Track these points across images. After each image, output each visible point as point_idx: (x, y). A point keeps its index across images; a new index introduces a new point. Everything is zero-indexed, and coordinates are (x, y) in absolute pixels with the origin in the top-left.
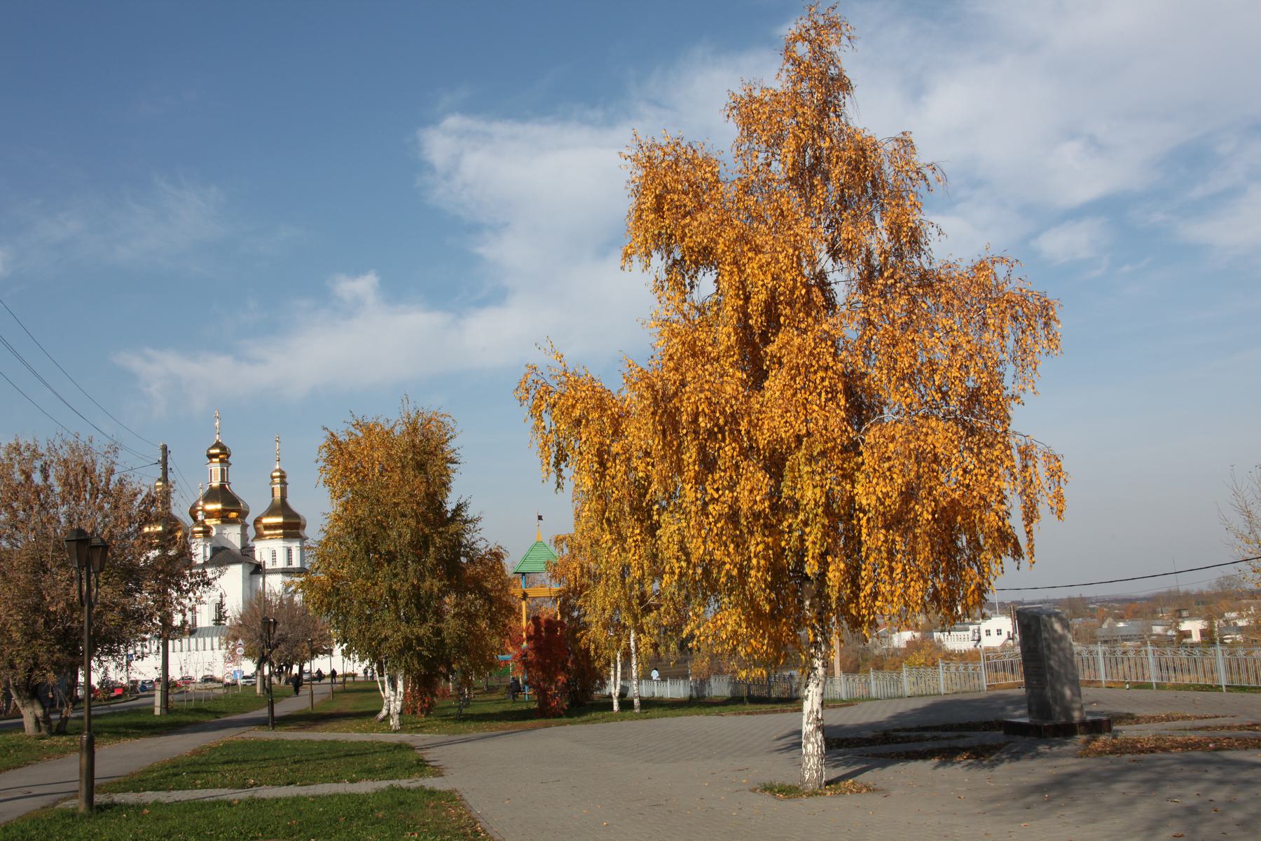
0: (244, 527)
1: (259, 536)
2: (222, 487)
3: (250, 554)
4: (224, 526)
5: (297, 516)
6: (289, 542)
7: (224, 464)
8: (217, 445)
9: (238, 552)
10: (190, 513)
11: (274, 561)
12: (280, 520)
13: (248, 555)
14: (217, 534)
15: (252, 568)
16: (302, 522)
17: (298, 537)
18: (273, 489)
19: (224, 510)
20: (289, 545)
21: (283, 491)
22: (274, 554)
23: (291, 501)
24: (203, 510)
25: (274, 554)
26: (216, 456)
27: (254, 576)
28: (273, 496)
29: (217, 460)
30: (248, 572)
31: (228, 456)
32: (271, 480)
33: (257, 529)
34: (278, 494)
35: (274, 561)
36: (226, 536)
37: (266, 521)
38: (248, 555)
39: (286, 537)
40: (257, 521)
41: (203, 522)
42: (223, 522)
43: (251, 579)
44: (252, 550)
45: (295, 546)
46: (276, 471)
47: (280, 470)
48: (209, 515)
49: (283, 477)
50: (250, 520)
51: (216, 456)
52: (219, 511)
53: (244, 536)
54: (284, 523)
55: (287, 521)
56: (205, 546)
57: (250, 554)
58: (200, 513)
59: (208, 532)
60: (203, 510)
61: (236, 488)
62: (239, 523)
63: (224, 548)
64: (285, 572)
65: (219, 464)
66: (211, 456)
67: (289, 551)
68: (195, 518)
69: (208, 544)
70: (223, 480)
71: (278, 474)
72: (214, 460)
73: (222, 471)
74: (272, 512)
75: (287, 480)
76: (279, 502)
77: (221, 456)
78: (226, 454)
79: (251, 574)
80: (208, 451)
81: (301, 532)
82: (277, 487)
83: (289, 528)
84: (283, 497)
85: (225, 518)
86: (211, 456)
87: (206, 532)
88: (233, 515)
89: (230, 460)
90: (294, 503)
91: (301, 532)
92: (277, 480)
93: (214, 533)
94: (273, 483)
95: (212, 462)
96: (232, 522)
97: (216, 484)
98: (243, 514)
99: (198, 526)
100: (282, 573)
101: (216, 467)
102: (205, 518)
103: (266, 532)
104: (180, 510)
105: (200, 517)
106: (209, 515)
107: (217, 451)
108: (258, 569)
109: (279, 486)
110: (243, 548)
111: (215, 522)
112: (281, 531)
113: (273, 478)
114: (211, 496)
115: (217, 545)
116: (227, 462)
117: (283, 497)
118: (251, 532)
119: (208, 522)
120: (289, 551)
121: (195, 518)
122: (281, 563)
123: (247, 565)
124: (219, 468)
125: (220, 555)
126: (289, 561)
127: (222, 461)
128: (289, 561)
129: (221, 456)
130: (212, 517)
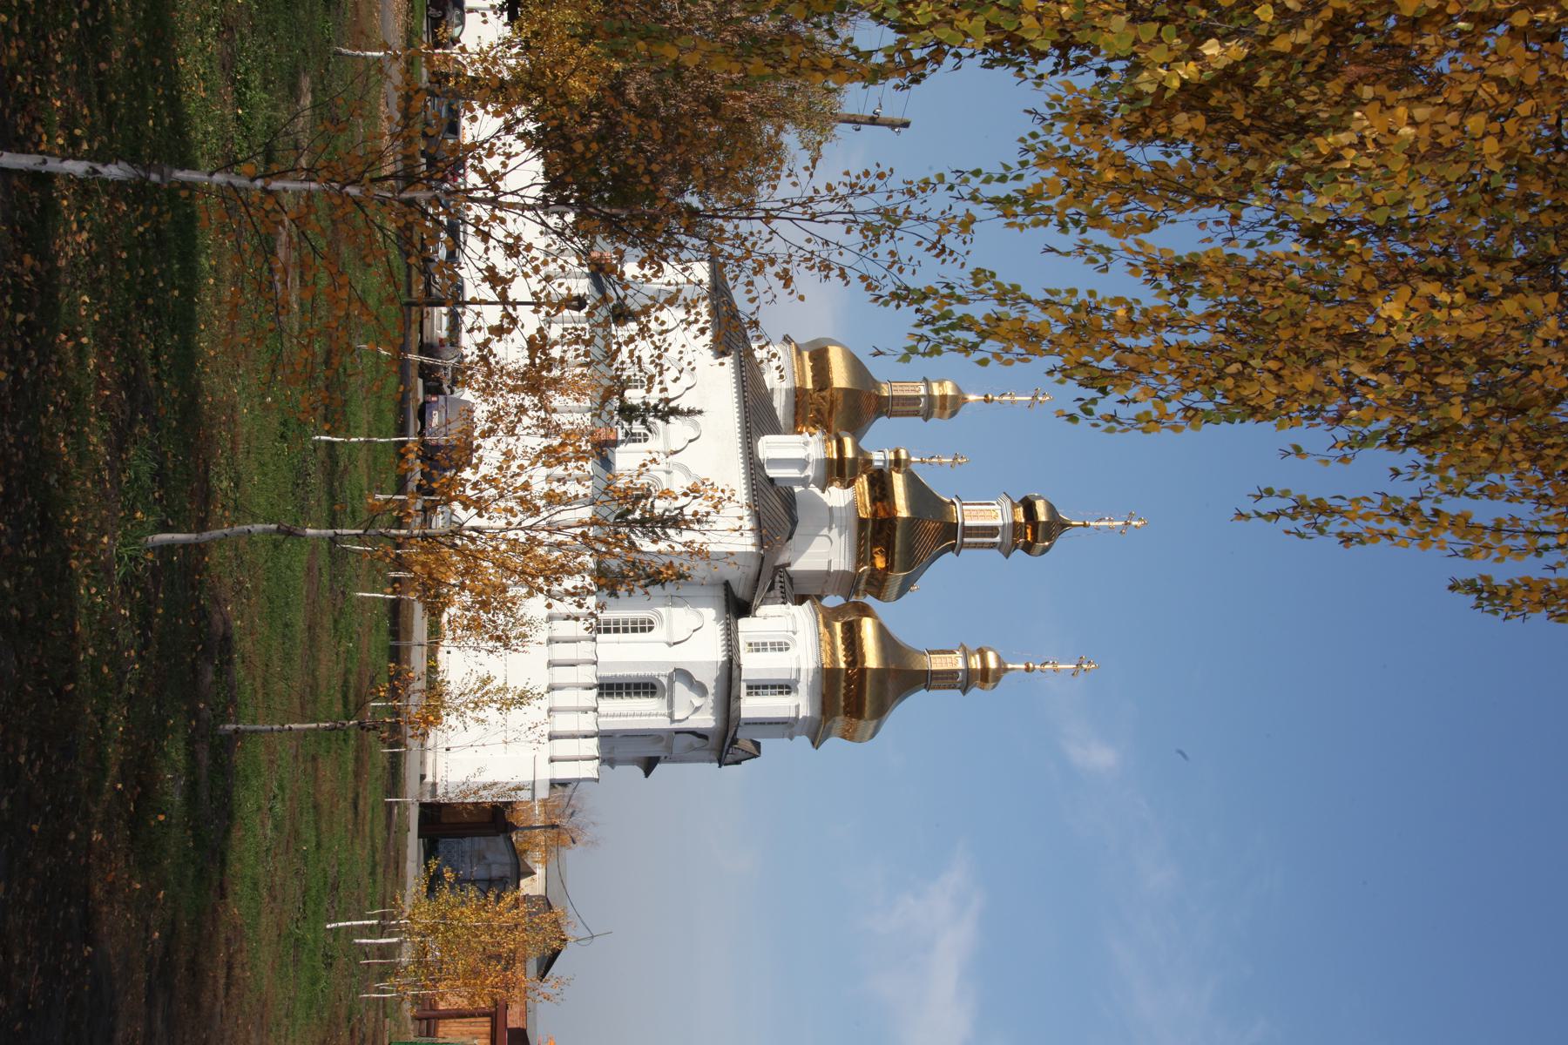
1: (829, 616)
3: (777, 592)
4: (853, 524)
5: (881, 711)
6: (812, 689)
7: (1009, 534)
11: (758, 647)
12: (872, 660)
13: (771, 588)
14: (831, 509)
15: (740, 591)
16: (866, 725)
18: (952, 652)
20: (803, 687)
21: (945, 679)
22: (782, 647)
23: (919, 701)
27: (722, 593)
30: (732, 573)
31: (1028, 548)
32: (972, 647)
34: (938, 663)
36: (825, 531)
37: (868, 628)
38: (771, 588)
39: (828, 677)
42: (862, 523)
43: (713, 584)
45: (799, 705)
47: (1002, 670)
48: (880, 485)
54: (863, 671)
55: (868, 673)
56: (802, 464)
57: (777, 592)
61: (943, 572)
62: (857, 568)
64: (730, 670)
65: (1008, 520)
66: (1029, 506)
67: (785, 688)
69: (810, 472)
71: (992, 664)
72: (1020, 510)
73: (991, 531)
74: (885, 639)
76: (918, 668)
78: (1035, 539)
79: (727, 584)
81: (840, 721)
82: (955, 662)
83: (849, 679)
86: (1029, 506)
87: (837, 471)
89: (1019, 553)
90: (915, 707)
91: (840, 721)
92: (975, 663)
93: (837, 497)
95: (1014, 506)
96: (861, 556)
101: (998, 514)
103: (838, 626)
106: (880, 485)
107: (1042, 516)
108: (737, 607)
109: (960, 665)
113: (982, 653)
115: (800, 513)
118: (834, 601)
119: (863, 483)
120: (785, 688)
122: (753, 665)
124: (999, 522)
125: (776, 502)
126: (756, 688)
128: (756, 688)
130: (874, 500)
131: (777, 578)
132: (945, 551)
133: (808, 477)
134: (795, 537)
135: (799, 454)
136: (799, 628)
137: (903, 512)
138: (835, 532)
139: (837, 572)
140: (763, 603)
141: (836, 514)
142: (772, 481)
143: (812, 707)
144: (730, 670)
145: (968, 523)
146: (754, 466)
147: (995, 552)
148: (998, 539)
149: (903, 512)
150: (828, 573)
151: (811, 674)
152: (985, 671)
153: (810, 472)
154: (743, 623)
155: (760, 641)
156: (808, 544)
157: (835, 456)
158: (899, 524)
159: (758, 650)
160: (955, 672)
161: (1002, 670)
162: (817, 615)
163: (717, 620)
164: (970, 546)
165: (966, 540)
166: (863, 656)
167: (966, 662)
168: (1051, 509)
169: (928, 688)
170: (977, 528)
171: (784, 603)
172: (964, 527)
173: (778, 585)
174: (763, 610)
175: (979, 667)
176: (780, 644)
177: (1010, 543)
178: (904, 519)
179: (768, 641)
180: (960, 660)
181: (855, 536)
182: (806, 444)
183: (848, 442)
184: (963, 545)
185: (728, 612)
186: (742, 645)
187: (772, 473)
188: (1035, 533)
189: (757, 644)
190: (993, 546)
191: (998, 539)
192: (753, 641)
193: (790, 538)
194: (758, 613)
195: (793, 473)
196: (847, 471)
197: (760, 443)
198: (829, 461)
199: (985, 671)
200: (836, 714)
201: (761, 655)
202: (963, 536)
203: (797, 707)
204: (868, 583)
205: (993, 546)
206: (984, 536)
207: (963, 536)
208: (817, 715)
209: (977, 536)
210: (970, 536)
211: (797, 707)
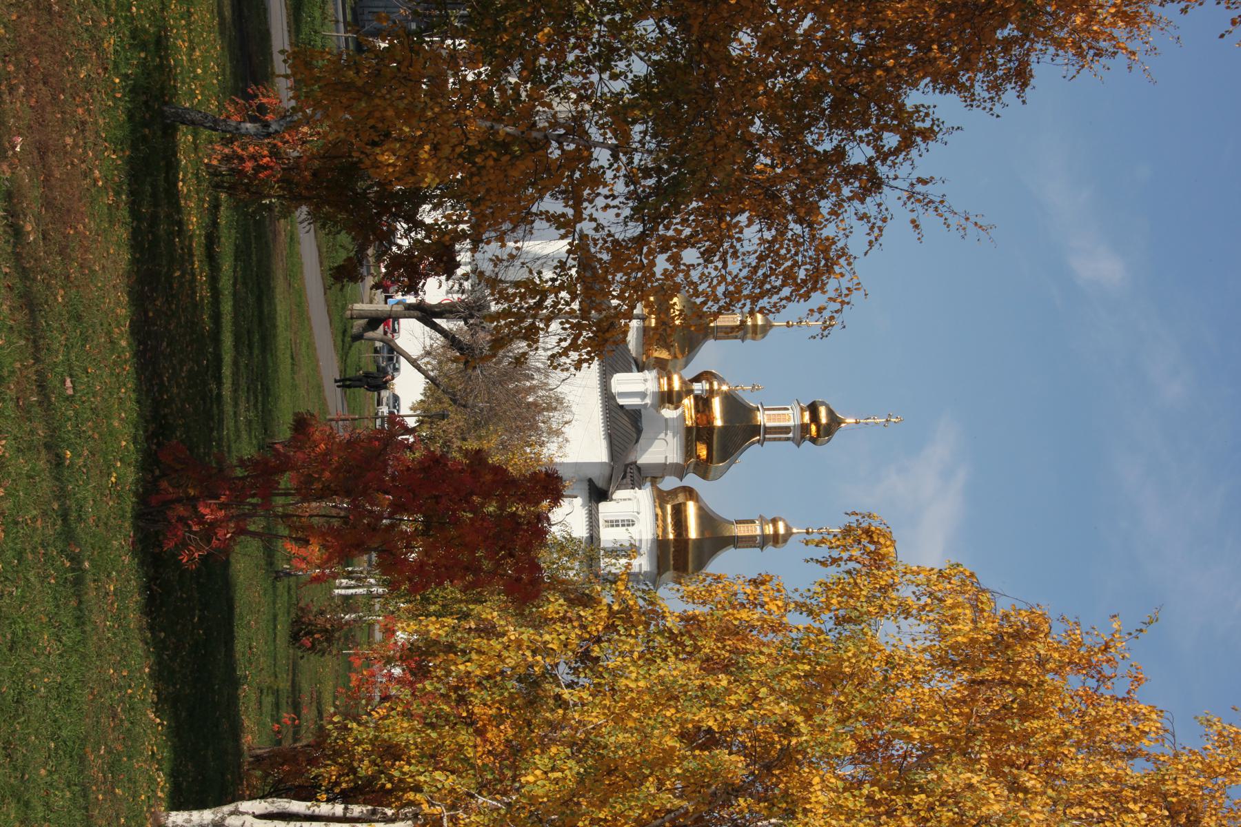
0: (679, 471)
2: (756, 429)
3: (628, 480)
4: (683, 432)
5: (700, 565)
6: (650, 552)
8: (835, 422)
9: (631, 459)
10: (706, 373)
11: (614, 524)
12: (693, 533)
13: (624, 477)
14: (666, 420)
15: (600, 484)
17: (659, 567)
18: (753, 522)
19: (710, 429)
21: (749, 541)
22: (630, 523)
24: (711, 392)
25: (630, 523)
26: (815, 417)
27: (586, 486)
28: (738, 522)
29: (807, 418)
30: (595, 475)
31: (813, 440)
32: (769, 518)
33: (674, 492)
34: (741, 531)
35: (614, 524)
36: (662, 436)
37: (691, 509)
38: (624, 477)
39: (660, 545)
40: (690, 493)
41: (690, 392)
43: (581, 480)
44: (636, 484)
46: (788, 528)
47: (789, 533)
48: (703, 404)
49: (776, 539)
50: (692, 480)
51: (815, 417)
52: (710, 420)
53: (664, 469)
54: (687, 540)
56: (643, 395)
57: (628, 480)
58: (707, 387)
59: (670, 402)
60: (711, 392)
61: (752, 456)
62: (686, 461)
63: (639, 431)
65: (798, 422)
66: (813, 409)
68: (697, 379)
69: (648, 401)
70: (768, 430)
71: (782, 530)
73: (786, 430)
74: (706, 518)
75: (770, 549)
76: (728, 534)
77: (813, 428)
78: (818, 435)
79: (590, 481)
80: (823, 403)
81: (669, 574)
82: (755, 530)
84: (736, 542)
85: (698, 433)
86: (813, 409)
87: (669, 398)
88: (703, 452)
89: (807, 444)
91: (669, 574)
92: (769, 530)
93: (669, 413)
94: (763, 521)
95: (802, 410)
96: (689, 450)
97: (762, 418)
98: (703, 469)
99: (683, 382)
100: (591, 537)
101: (792, 417)
102: (697, 398)
103: (669, 508)
104: (710, 355)
105: (697, 387)
106: (703, 404)
107: (824, 419)
108: (598, 494)
109: (758, 532)
110: (639, 468)
111: (687, 416)
112: (671, 536)
113: (774, 521)
114: (734, 405)
115: (645, 424)
116: (803, 438)
117: (736, 542)
118: (669, 483)
119: (688, 402)
121: (697, 379)
122: (608, 536)
123: (607, 472)
124: (791, 423)
125: (625, 421)
126: (614, 553)
127: (804, 428)
129: (813, 428)
130: (697, 411)
131: (629, 470)
132: (753, 443)
133: (646, 404)
134: (641, 441)
135: (640, 388)
136: (642, 510)
137: (718, 422)
138: (670, 434)
139: (672, 464)
140: (618, 488)
141: (670, 423)
142: (622, 407)
143: (651, 565)
144: (593, 538)
145: (769, 424)
146: (608, 397)
147: (790, 443)
148: (791, 435)
149: (718, 422)
150: (665, 464)
151: (649, 543)
152: (776, 535)
153: (648, 401)
154: (605, 508)
155: (614, 519)
156: (650, 445)
157: (666, 389)
158: (716, 431)
159: (612, 526)
160: (755, 537)
161: (789, 533)
162: (655, 502)
163: (583, 506)
164: (770, 439)
165: (767, 436)
166: (687, 530)
167: (762, 530)
168: (830, 413)
169: (736, 547)
170: (775, 428)
171: (633, 488)
172: (765, 428)
173: (628, 475)
174: (620, 494)
175: (772, 532)
176: (628, 521)
177: (799, 438)
178: (719, 427)
179: (620, 518)
180: (758, 528)
181: (683, 438)
182: (646, 380)
183: (676, 378)
184: (765, 439)
185: (590, 501)
186: (601, 522)
187: (621, 401)
188: (818, 430)
189: (612, 521)
190: (788, 439)
191: (791, 435)
192: (610, 519)
193: (637, 441)
194: (614, 497)
195: (636, 401)
196: (675, 400)
197: (612, 381)
198: (662, 393)
199: (776, 535)
200: (667, 570)
201: (615, 529)
202: (765, 433)
203: (640, 565)
204: (695, 468)
205: (788, 439)
206: (781, 433)
207: (765, 433)
208: (655, 571)
209: (775, 433)
210: (770, 433)
211: (640, 565)
